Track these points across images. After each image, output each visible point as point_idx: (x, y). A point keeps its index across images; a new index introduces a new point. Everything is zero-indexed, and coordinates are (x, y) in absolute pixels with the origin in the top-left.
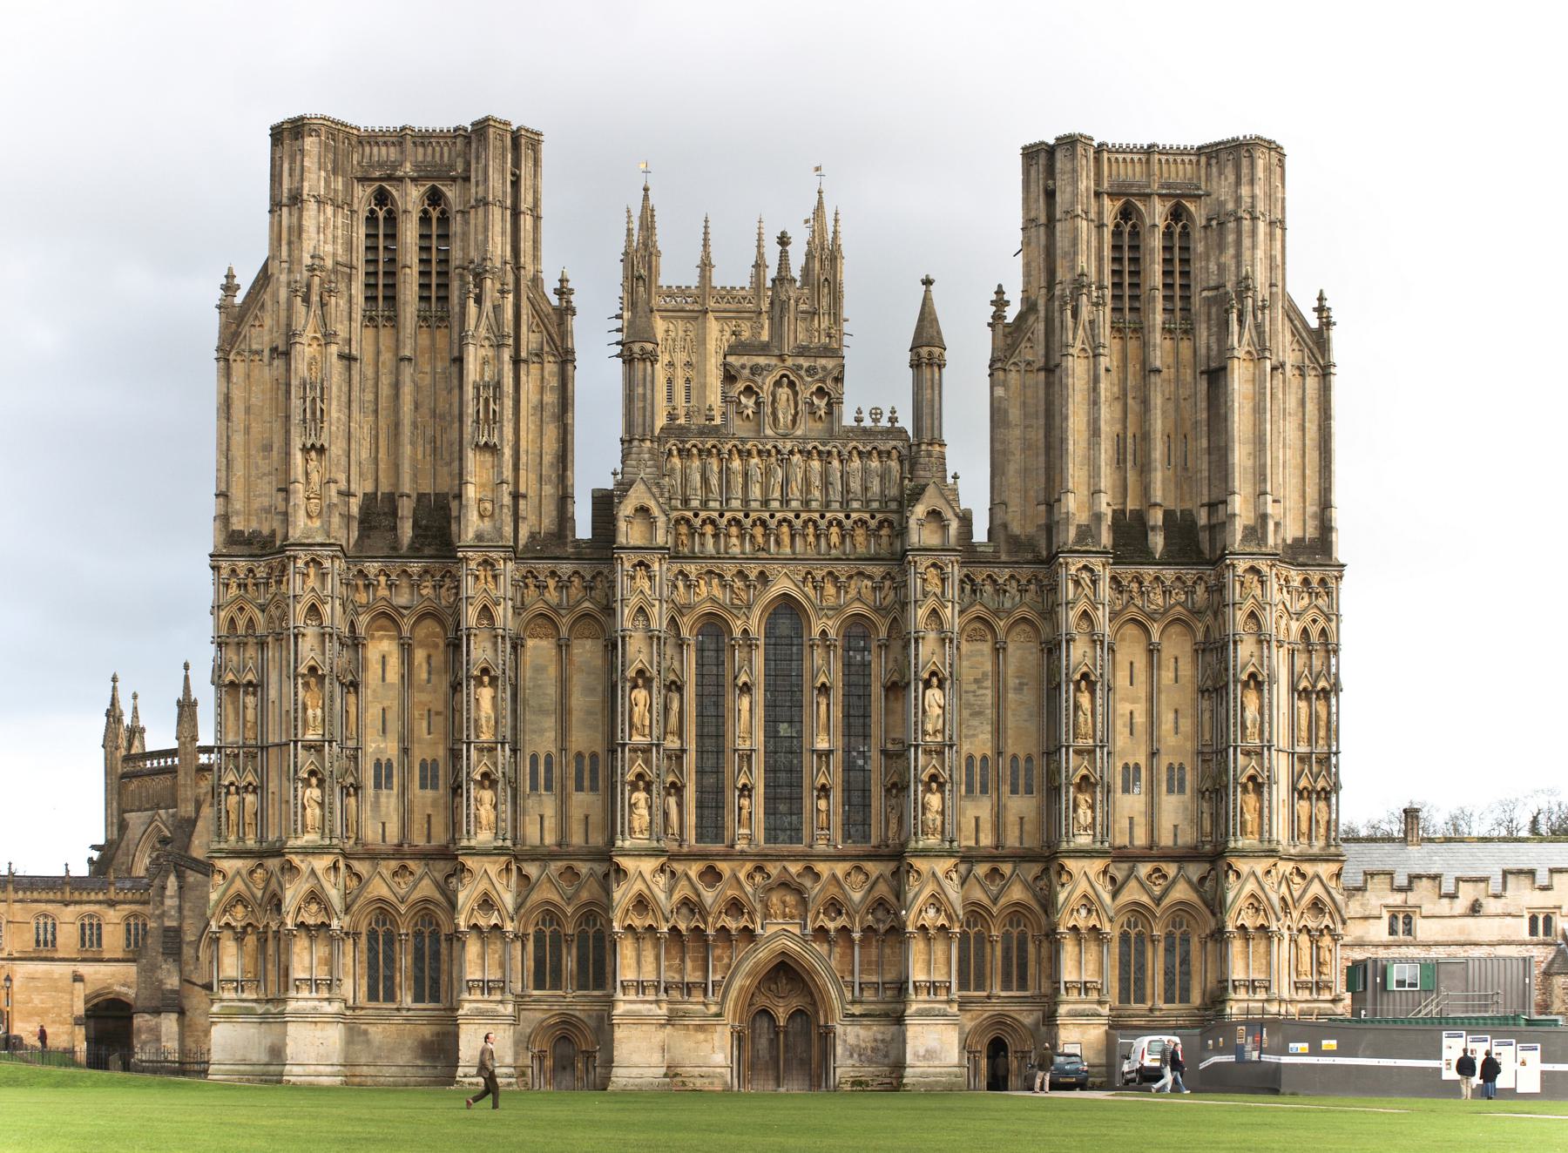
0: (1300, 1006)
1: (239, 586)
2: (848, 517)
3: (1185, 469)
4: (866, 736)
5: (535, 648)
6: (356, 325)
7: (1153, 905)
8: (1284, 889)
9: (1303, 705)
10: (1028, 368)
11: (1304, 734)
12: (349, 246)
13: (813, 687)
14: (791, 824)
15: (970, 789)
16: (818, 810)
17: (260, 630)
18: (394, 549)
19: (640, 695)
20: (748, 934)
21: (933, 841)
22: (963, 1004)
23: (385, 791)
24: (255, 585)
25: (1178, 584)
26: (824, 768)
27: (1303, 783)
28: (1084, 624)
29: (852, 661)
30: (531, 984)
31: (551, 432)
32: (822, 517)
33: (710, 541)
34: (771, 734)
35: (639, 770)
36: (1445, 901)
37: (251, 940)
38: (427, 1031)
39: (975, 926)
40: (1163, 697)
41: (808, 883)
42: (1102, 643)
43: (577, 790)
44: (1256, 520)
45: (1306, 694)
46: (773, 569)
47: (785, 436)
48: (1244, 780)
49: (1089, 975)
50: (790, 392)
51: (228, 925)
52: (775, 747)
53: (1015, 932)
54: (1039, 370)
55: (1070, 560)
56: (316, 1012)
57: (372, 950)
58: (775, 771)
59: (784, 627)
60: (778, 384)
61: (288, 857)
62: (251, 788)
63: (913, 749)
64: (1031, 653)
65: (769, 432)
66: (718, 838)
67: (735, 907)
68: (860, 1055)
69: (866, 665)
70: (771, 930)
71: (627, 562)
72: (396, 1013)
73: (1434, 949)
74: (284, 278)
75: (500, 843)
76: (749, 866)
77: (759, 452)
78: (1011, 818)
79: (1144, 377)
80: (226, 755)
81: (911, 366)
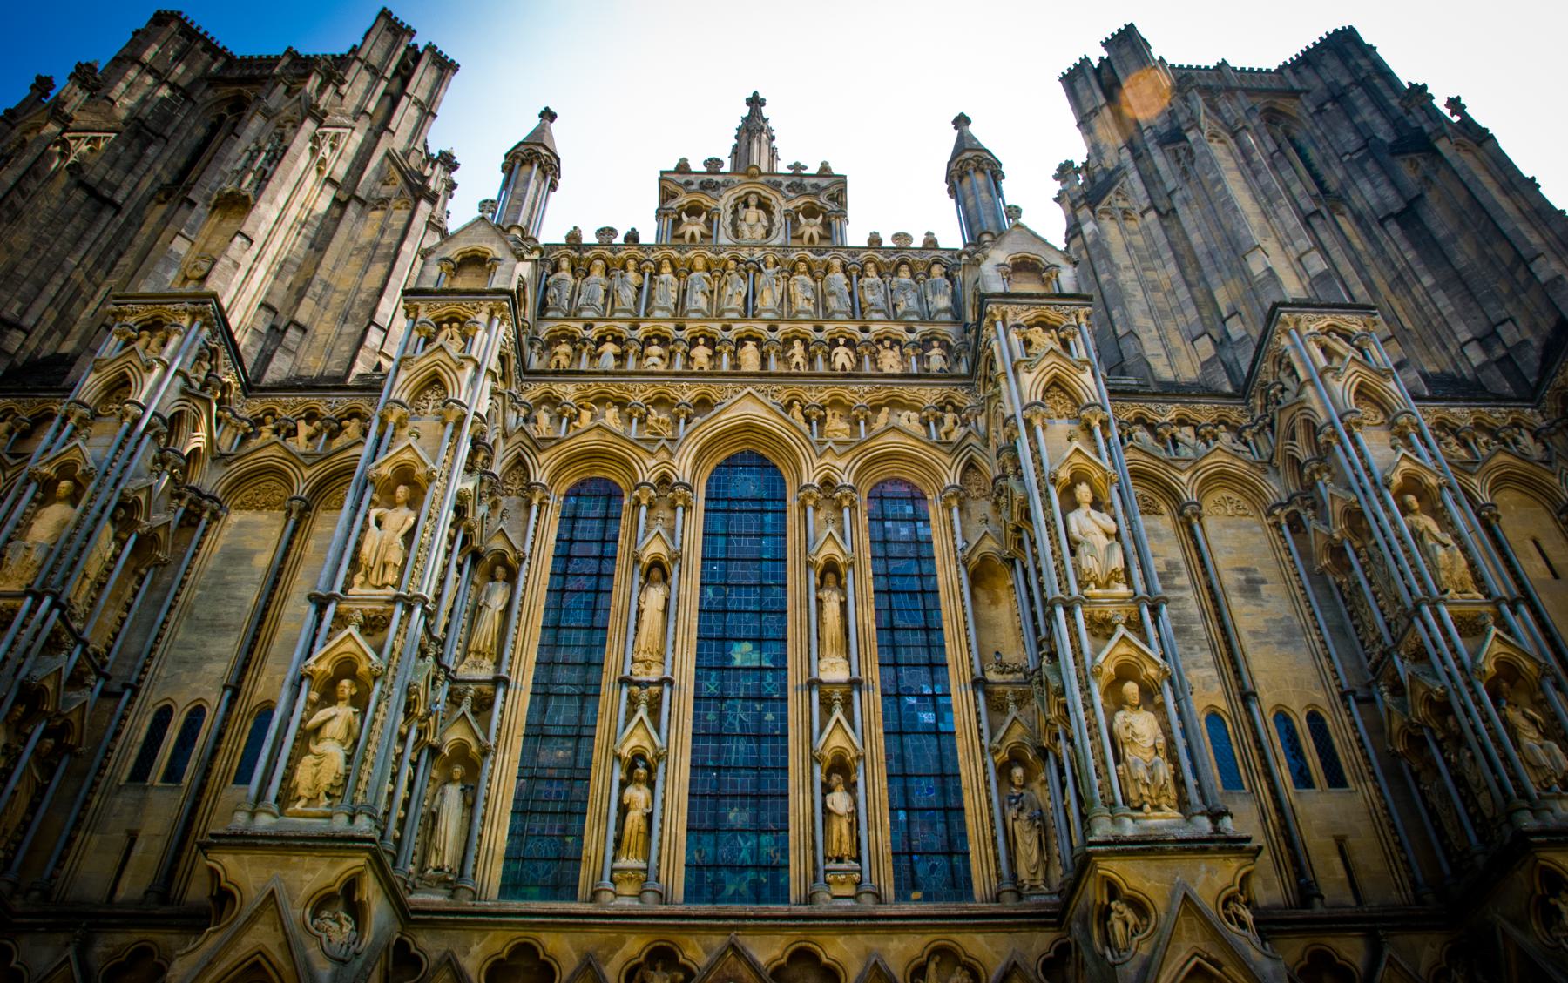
2: (865, 330)
4: (936, 666)
5: (241, 525)
13: (809, 565)
14: (756, 851)
16: (827, 812)
26: (838, 713)
29: (891, 536)
33: (608, 362)
35: (349, 647)
50: (761, 212)
52: (723, 688)
54: (1142, 214)
55: (1303, 317)
58: (719, 736)
63: (1060, 612)
64: (1255, 534)
76: (635, 946)
78: (1315, 840)
81: (953, 192)
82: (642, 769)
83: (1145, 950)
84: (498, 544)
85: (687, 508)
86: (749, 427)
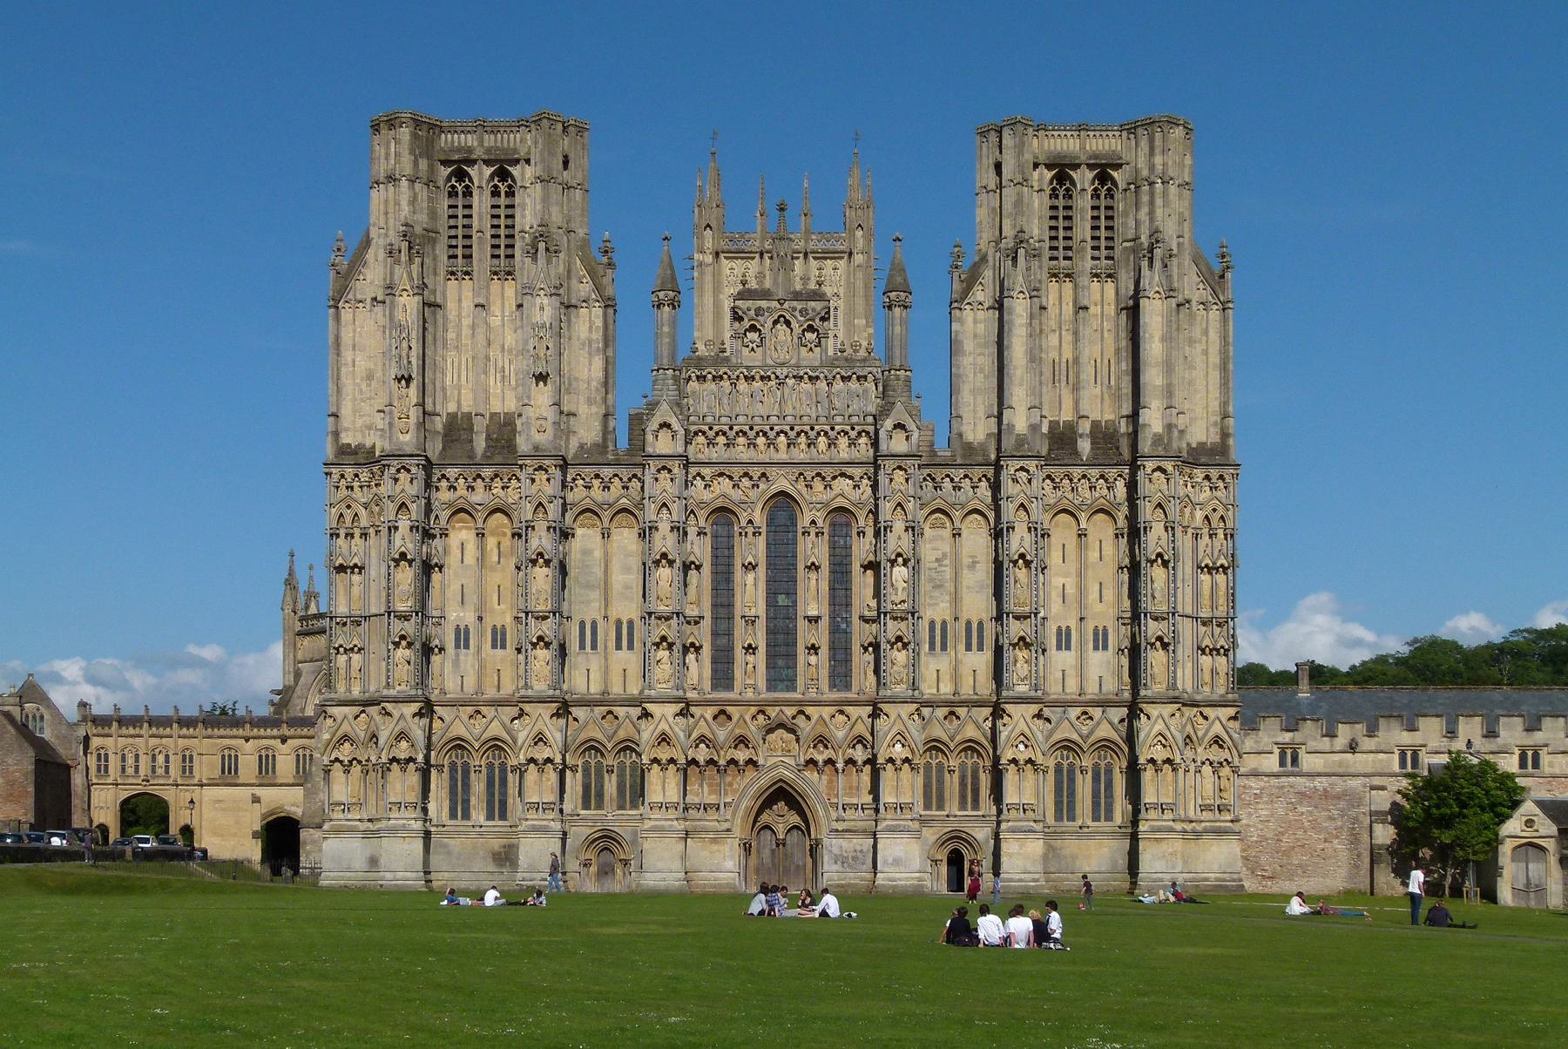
0: (1203, 824)
1: (347, 488)
2: (833, 429)
3: (1109, 387)
4: (848, 605)
5: (583, 536)
6: (441, 278)
7: (1081, 741)
8: (1189, 729)
9: (1205, 578)
10: (980, 307)
11: (1206, 601)
12: (433, 214)
14: (787, 676)
15: (932, 647)
17: (364, 522)
18: (471, 457)
19: (664, 573)
20: (751, 762)
21: (900, 689)
22: (923, 821)
23: (464, 651)
24: (361, 487)
25: (1101, 481)
27: (1207, 642)
28: (1022, 513)
30: (580, 806)
31: (598, 363)
32: (812, 429)
33: (720, 448)
34: (771, 603)
36: (1326, 739)
37: (356, 770)
38: (496, 844)
39: (937, 758)
40: (1090, 572)
41: (801, 720)
42: (1036, 529)
43: (617, 649)
44: (1164, 428)
45: (1210, 570)
46: (772, 472)
47: (782, 365)
48: (1153, 640)
49: (1028, 798)
51: (337, 760)
53: (969, 762)
56: (404, 828)
57: (453, 779)
59: (782, 517)
60: (776, 322)
61: (383, 704)
62: (356, 649)
65: (769, 362)
66: (730, 687)
67: (742, 741)
68: (843, 863)
69: (848, 548)
70: (771, 761)
71: (654, 465)
72: (471, 829)
73: (1319, 779)
74: (382, 242)
75: (551, 692)
76: (753, 710)
77: (762, 378)
78: (966, 672)
79: (1076, 313)
80: (338, 623)
82: (751, 649)
83: (886, 728)
84: (692, 558)
85: (760, 533)
86: (782, 493)
